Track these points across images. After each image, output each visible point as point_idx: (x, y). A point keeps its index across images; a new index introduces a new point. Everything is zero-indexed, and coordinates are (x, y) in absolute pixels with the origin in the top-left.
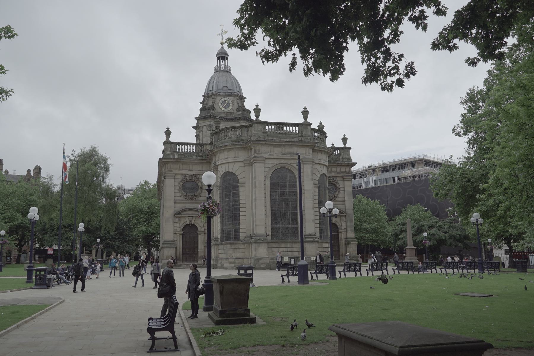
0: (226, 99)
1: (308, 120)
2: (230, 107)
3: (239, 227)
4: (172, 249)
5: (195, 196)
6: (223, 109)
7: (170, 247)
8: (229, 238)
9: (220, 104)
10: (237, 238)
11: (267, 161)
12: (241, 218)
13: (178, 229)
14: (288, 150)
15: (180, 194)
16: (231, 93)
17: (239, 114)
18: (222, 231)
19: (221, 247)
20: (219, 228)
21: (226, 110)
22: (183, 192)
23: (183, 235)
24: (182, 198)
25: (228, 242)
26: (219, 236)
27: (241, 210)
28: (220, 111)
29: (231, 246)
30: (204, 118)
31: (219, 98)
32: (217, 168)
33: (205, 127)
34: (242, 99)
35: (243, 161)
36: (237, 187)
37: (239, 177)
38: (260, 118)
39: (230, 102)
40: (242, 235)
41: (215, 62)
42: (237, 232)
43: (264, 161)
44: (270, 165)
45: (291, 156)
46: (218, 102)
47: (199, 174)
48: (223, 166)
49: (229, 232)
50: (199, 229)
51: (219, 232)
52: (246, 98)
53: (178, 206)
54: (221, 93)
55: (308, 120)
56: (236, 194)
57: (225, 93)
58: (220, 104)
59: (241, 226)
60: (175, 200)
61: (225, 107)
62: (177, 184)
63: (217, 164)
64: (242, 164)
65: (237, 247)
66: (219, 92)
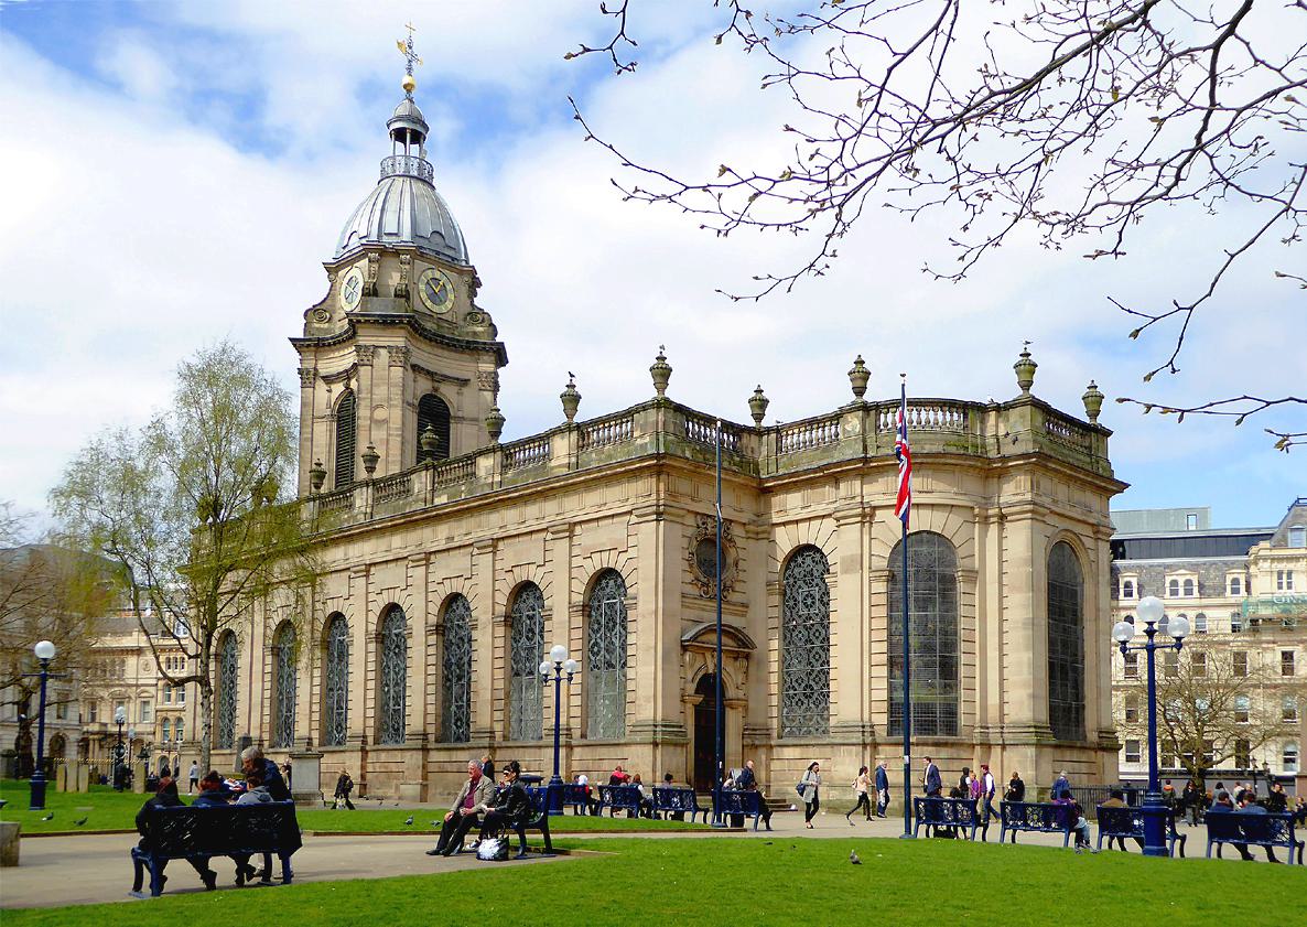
0: (437, 275)
1: (1100, 420)
2: (449, 305)
3: (954, 695)
4: (679, 749)
5: (726, 588)
6: (429, 304)
7: (676, 745)
8: (927, 727)
9: (422, 287)
10: (951, 726)
11: (1051, 519)
14: (1079, 495)
15: (690, 577)
16: (453, 259)
20: (884, 695)
21: (436, 309)
22: (696, 570)
23: (697, 707)
24: (694, 591)
25: (930, 738)
26: (882, 719)
27: (963, 646)
28: (421, 308)
29: (938, 752)
30: (384, 323)
32: (872, 516)
33: (383, 352)
34: (475, 284)
39: (449, 287)
42: (951, 713)
43: (1044, 515)
44: (1049, 532)
45: (1083, 514)
46: (416, 277)
47: (731, 521)
48: (925, 513)
49: (926, 709)
50: (731, 692)
51: (884, 706)
52: (479, 285)
54: (427, 252)
57: (438, 253)
58: (422, 287)
60: (684, 596)
63: (873, 504)
65: (955, 756)
66: (421, 247)
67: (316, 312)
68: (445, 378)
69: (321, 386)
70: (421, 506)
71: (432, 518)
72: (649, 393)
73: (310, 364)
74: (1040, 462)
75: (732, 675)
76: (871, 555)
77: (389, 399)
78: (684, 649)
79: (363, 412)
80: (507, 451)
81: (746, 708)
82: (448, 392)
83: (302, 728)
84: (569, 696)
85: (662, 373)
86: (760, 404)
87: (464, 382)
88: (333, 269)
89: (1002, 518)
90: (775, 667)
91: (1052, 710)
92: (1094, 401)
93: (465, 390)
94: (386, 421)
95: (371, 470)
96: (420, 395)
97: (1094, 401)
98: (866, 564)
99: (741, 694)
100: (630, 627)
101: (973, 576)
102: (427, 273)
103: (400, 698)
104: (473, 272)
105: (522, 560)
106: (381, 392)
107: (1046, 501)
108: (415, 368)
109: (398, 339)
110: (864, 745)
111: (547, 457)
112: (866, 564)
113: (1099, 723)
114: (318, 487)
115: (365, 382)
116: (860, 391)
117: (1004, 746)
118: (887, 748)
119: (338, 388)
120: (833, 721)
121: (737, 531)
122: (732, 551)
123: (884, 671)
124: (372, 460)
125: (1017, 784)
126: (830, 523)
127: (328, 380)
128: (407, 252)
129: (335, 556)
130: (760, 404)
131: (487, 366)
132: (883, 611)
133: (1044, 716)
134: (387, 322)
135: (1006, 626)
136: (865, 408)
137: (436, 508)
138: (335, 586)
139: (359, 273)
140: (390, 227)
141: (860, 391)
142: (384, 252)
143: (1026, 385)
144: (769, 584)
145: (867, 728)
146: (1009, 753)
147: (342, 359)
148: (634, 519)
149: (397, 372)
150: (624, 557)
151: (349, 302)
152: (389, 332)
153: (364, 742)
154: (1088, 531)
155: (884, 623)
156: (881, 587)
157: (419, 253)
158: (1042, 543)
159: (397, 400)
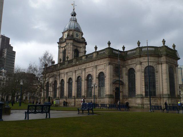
0: (77, 33)
10: (155, 95)
11: (169, 64)
12: (156, 86)
13: (114, 89)
17: (82, 40)
18: (146, 92)
19: (145, 99)
22: (115, 72)
23: (115, 93)
24: (114, 75)
26: (144, 94)
27: (156, 83)
31: (75, 32)
34: (82, 34)
35: (157, 62)
36: (154, 73)
37: (155, 69)
38: (165, 45)
40: (157, 94)
41: (71, 17)
42: (155, 92)
50: (121, 90)
53: (114, 78)
55: (176, 49)
56: (154, 76)
59: (157, 90)
61: (76, 36)
62: (113, 68)
64: (156, 63)
67: (61, 39)
68: (79, 47)
69: (61, 49)
70: (74, 64)
71: (76, 65)
72: (107, 46)
73: (60, 46)
74: (167, 55)
75: (121, 87)
76: (142, 69)
77: (70, 50)
78: (113, 83)
79: (67, 52)
80: (87, 56)
81: (123, 92)
82: (79, 49)
83: (58, 96)
84: (96, 91)
85: (109, 44)
86: (124, 48)
87: (81, 47)
88: (63, 33)
89: (161, 64)
90: (127, 86)
91: (170, 92)
92: (174, 46)
93: (81, 48)
94: (70, 53)
95: (68, 59)
96: (74, 49)
97: (174, 46)
98: (141, 71)
99: (122, 90)
100: (105, 80)
101: (157, 72)
102: (75, 33)
103: (71, 91)
104: (82, 33)
105: (89, 71)
106: (69, 49)
107: (168, 61)
108: (74, 46)
109: (72, 41)
110: (141, 98)
111: (92, 56)
112: (141, 71)
113: (177, 94)
114: (60, 62)
115: (67, 48)
116: (139, 45)
117: (163, 98)
118: (145, 98)
119: (64, 49)
120: (136, 94)
121: (121, 66)
122: (120, 69)
123: (144, 87)
124: (68, 58)
125: (166, 104)
126: (135, 65)
127: (62, 48)
128: (73, 30)
129: (62, 71)
130: (124, 48)
131: (84, 45)
132: (144, 78)
133: (169, 93)
134: (70, 39)
135: (163, 80)
136: (140, 48)
137: (77, 64)
138: (62, 76)
139: (66, 34)
140: (71, 27)
141: (139, 45)
142: (70, 30)
143: (164, 44)
144: (126, 74)
145: (141, 95)
146: (164, 99)
147: (64, 45)
148: (105, 65)
149: (72, 46)
150: (104, 70)
151: (65, 37)
152: (70, 41)
153: (66, 98)
154: (175, 65)
155: (144, 79)
156: (143, 74)
157: (75, 30)
158: (168, 67)
159: (71, 50)
